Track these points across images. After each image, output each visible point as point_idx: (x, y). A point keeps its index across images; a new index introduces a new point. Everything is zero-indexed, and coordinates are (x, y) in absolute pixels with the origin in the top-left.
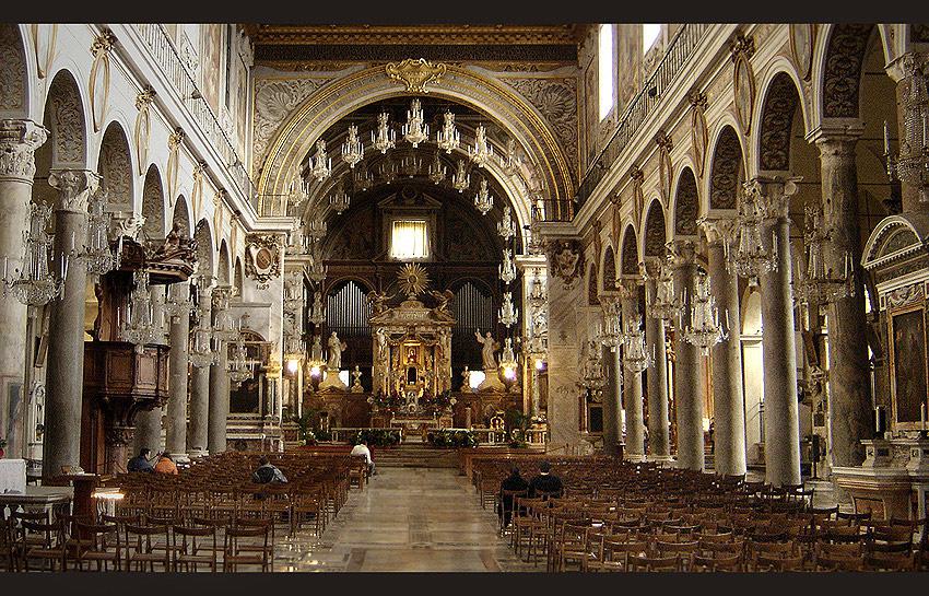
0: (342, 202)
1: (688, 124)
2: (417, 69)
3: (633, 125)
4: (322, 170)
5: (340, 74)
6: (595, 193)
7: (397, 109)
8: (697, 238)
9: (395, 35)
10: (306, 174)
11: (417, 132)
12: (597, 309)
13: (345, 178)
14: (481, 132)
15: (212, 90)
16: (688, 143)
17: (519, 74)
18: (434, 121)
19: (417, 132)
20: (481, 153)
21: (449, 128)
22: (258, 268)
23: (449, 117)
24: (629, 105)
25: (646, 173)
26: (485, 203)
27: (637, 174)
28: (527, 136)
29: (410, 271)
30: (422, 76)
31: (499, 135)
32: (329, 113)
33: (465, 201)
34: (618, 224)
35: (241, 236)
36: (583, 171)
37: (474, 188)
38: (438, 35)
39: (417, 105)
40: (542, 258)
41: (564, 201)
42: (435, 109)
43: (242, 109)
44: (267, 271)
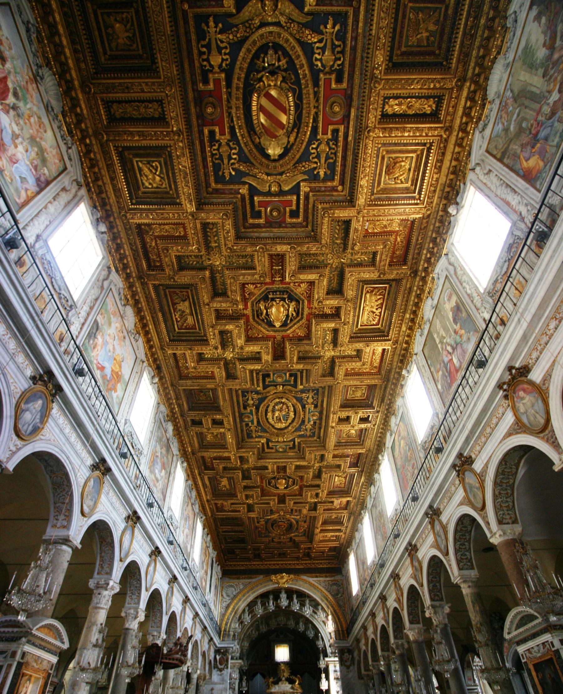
0: (255, 634)
1: (393, 588)
2: (282, 578)
3: (368, 594)
4: (247, 618)
5: (254, 580)
6: (356, 626)
7: (276, 594)
8: (404, 641)
9: (274, 564)
10: (242, 623)
11: (284, 602)
12: (362, 681)
13: (256, 624)
14: (307, 602)
15: (204, 584)
16: (394, 596)
17: (321, 579)
18: (290, 598)
19: (284, 602)
20: (308, 611)
21: (295, 600)
22: (220, 667)
23: (295, 596)
24: (365, 586)
25: (376, 613)
26: (311, 634)
27: (373, 615)
28: (326, 604)
29: (283, 667)
30: (284, 580)
31: (315, 605)
32: (249, 596)
33: (303, 635)
34: (367, 638)
35: (212, 650)
36: (349, 617)
37: (307, 629)
38: (290, 564)
39: (283, 592)
40: (337, 659)
41: (343, 631)
42: (290, 593)
43: (216, 595)
44: (222, 667)
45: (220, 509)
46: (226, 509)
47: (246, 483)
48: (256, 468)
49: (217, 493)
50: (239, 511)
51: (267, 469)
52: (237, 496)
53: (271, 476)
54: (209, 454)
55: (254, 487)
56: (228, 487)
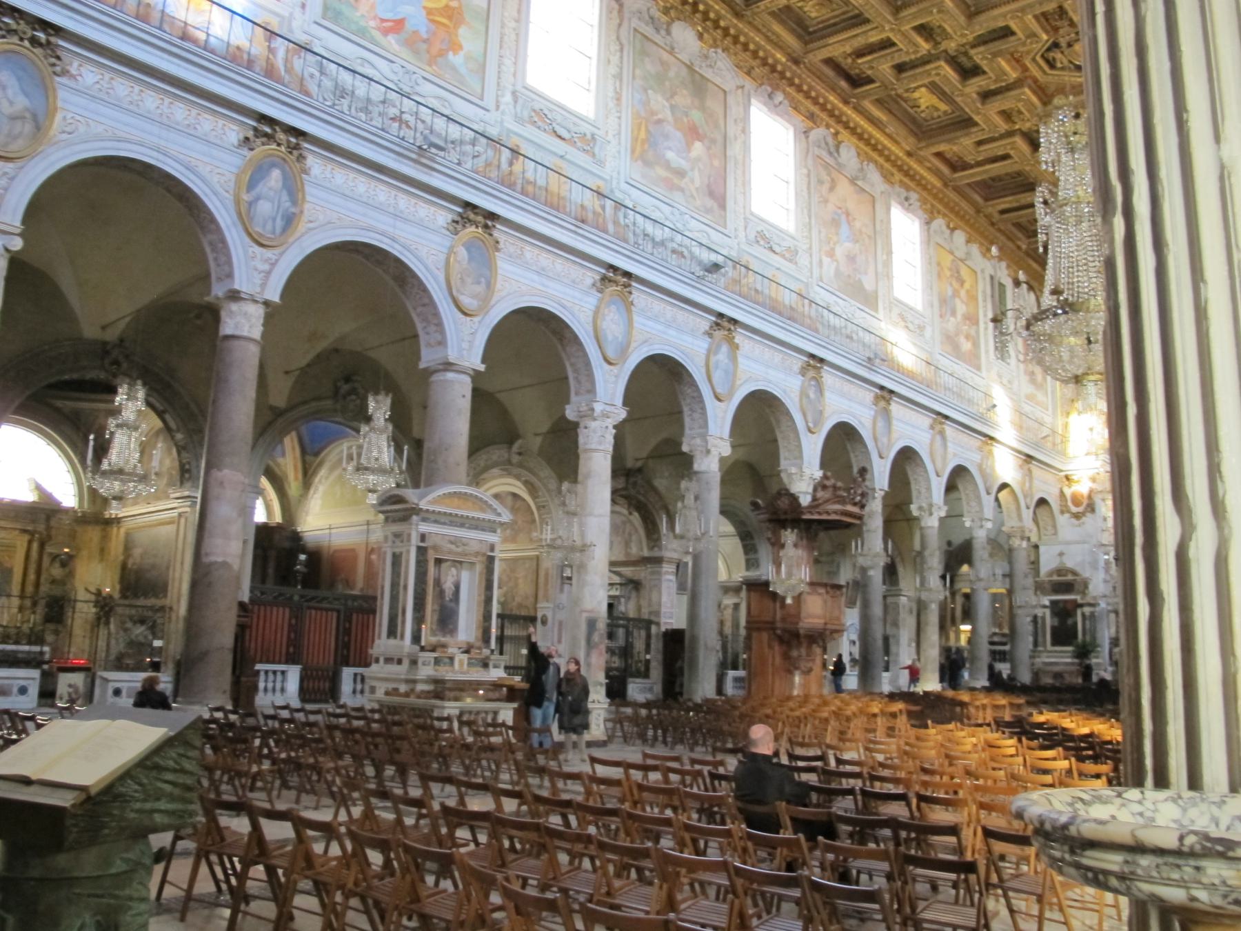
45: (957, 165)
46: (970, 159)
47: (977, 84)
48: (983, 41)
49: (922, 130)
50: (1005, 157)
51: (1013, 33)
52: (976, 124)
53: (1037, 47)
54: (839, 47)
55: (1008, 88)
56: (943, 107)
